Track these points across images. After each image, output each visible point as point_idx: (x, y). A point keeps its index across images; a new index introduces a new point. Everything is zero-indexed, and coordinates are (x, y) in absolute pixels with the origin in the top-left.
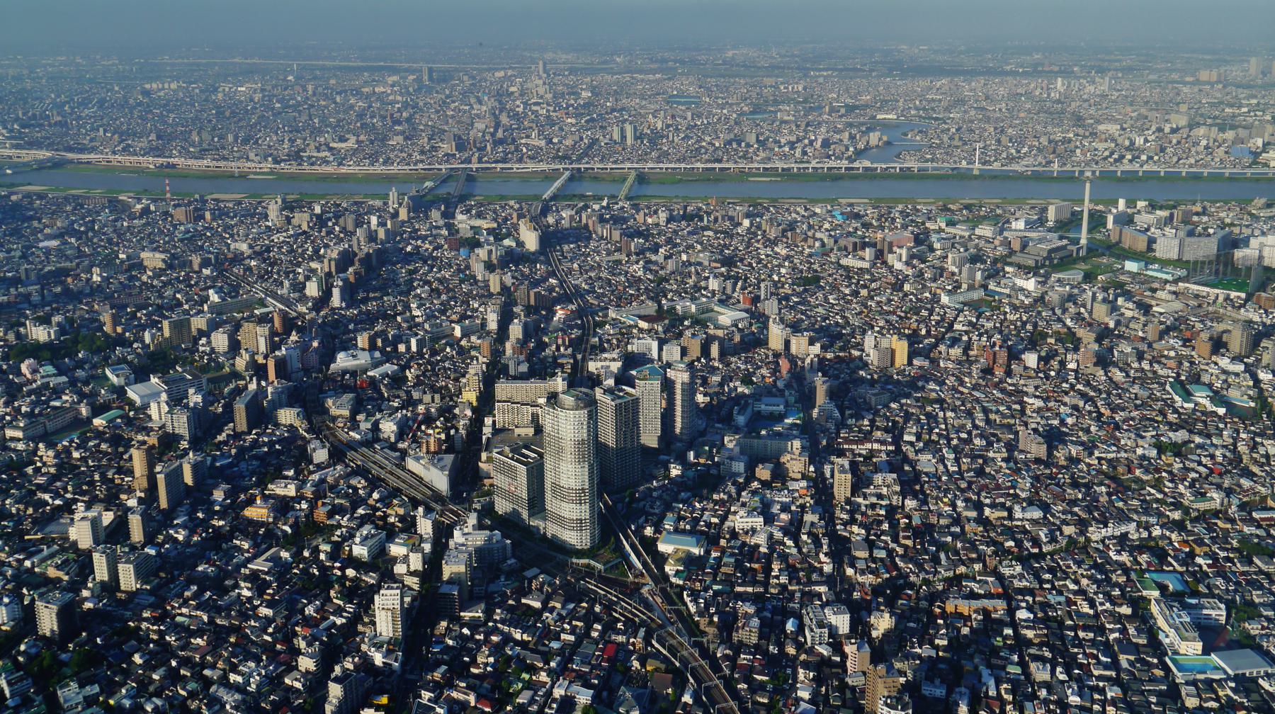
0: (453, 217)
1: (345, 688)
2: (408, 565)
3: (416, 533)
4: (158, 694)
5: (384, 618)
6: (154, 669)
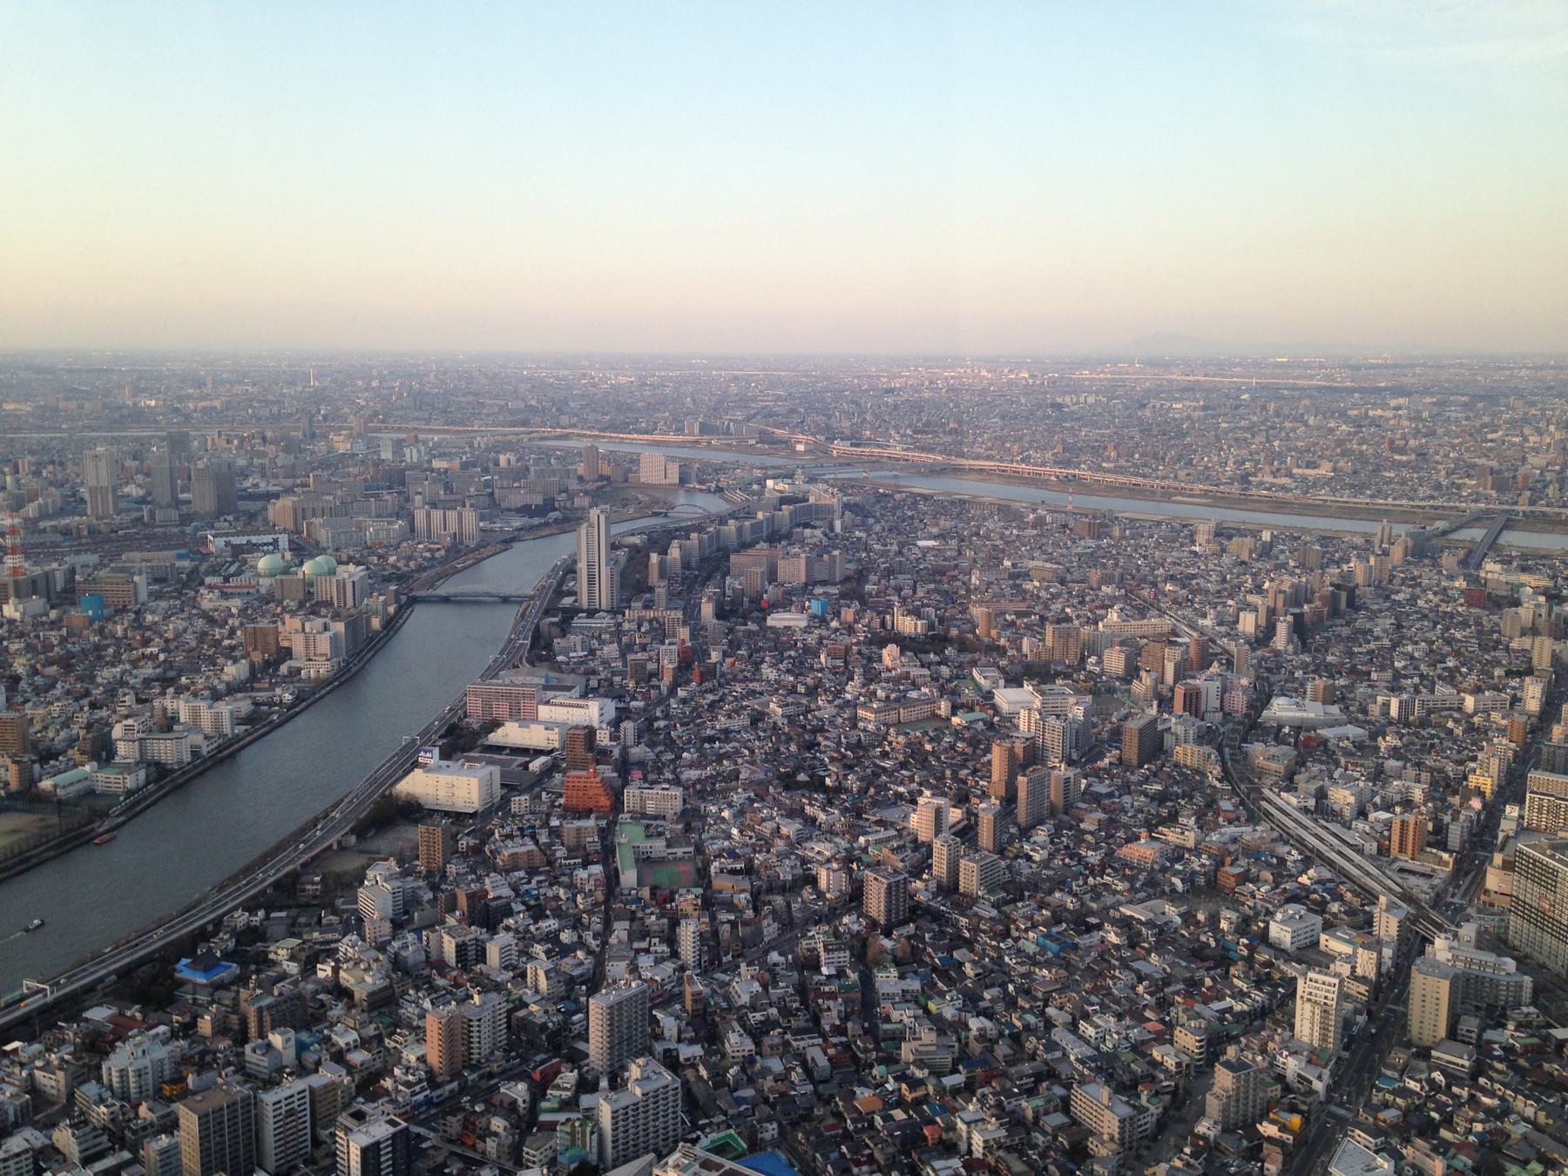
0: (1479, 566)
1: (1238, 1079)
2: (1354, 968)
3: (1370, 933)
4: (988, 1014)
5: (1308, 1014)
6: (987, 987)
